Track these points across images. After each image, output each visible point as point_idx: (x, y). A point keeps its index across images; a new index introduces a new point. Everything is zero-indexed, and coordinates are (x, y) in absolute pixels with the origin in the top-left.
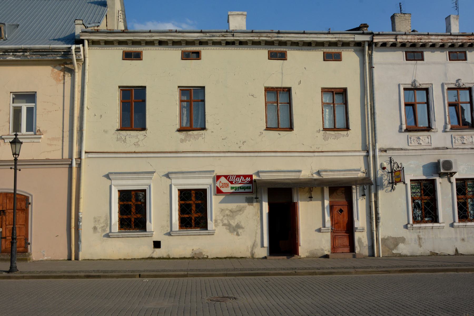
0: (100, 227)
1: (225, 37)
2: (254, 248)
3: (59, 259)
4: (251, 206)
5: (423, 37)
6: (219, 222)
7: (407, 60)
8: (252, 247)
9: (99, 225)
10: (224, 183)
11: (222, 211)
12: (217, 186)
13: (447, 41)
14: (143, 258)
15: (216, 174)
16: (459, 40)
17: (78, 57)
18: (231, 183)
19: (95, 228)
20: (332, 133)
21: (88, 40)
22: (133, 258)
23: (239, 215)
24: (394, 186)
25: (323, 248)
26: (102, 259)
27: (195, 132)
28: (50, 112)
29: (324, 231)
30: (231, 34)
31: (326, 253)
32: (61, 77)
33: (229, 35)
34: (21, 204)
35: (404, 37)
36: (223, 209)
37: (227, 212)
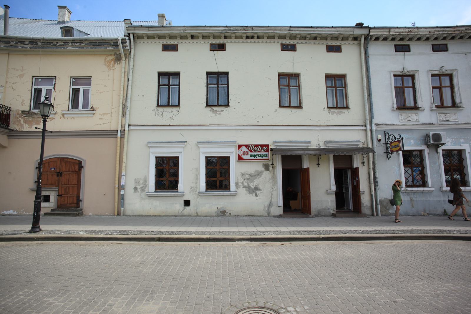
0: (140, 187)
1: (246, 30)
2: (270, 207)
4: (267, 171)
5: (413, 29)
6: (240, 185)
7: (396, 51)
8: (268, 206)
9: (139, 186)
10: (245, 152)
13: (434, 33)
16: (445, 32)
18: (251, 151)
19: (135, 188)
20: (335, 110)
21: (133, 34)
23: (257, 179)
24: (390, 155)
25: (330, 208)
29: (330, 193)
30: (251, 28)
31: (332, 212)
33: (249, 29)
34: (74, 167)
35: (397, 30)
36: (243, 173)
37: (247, 176)
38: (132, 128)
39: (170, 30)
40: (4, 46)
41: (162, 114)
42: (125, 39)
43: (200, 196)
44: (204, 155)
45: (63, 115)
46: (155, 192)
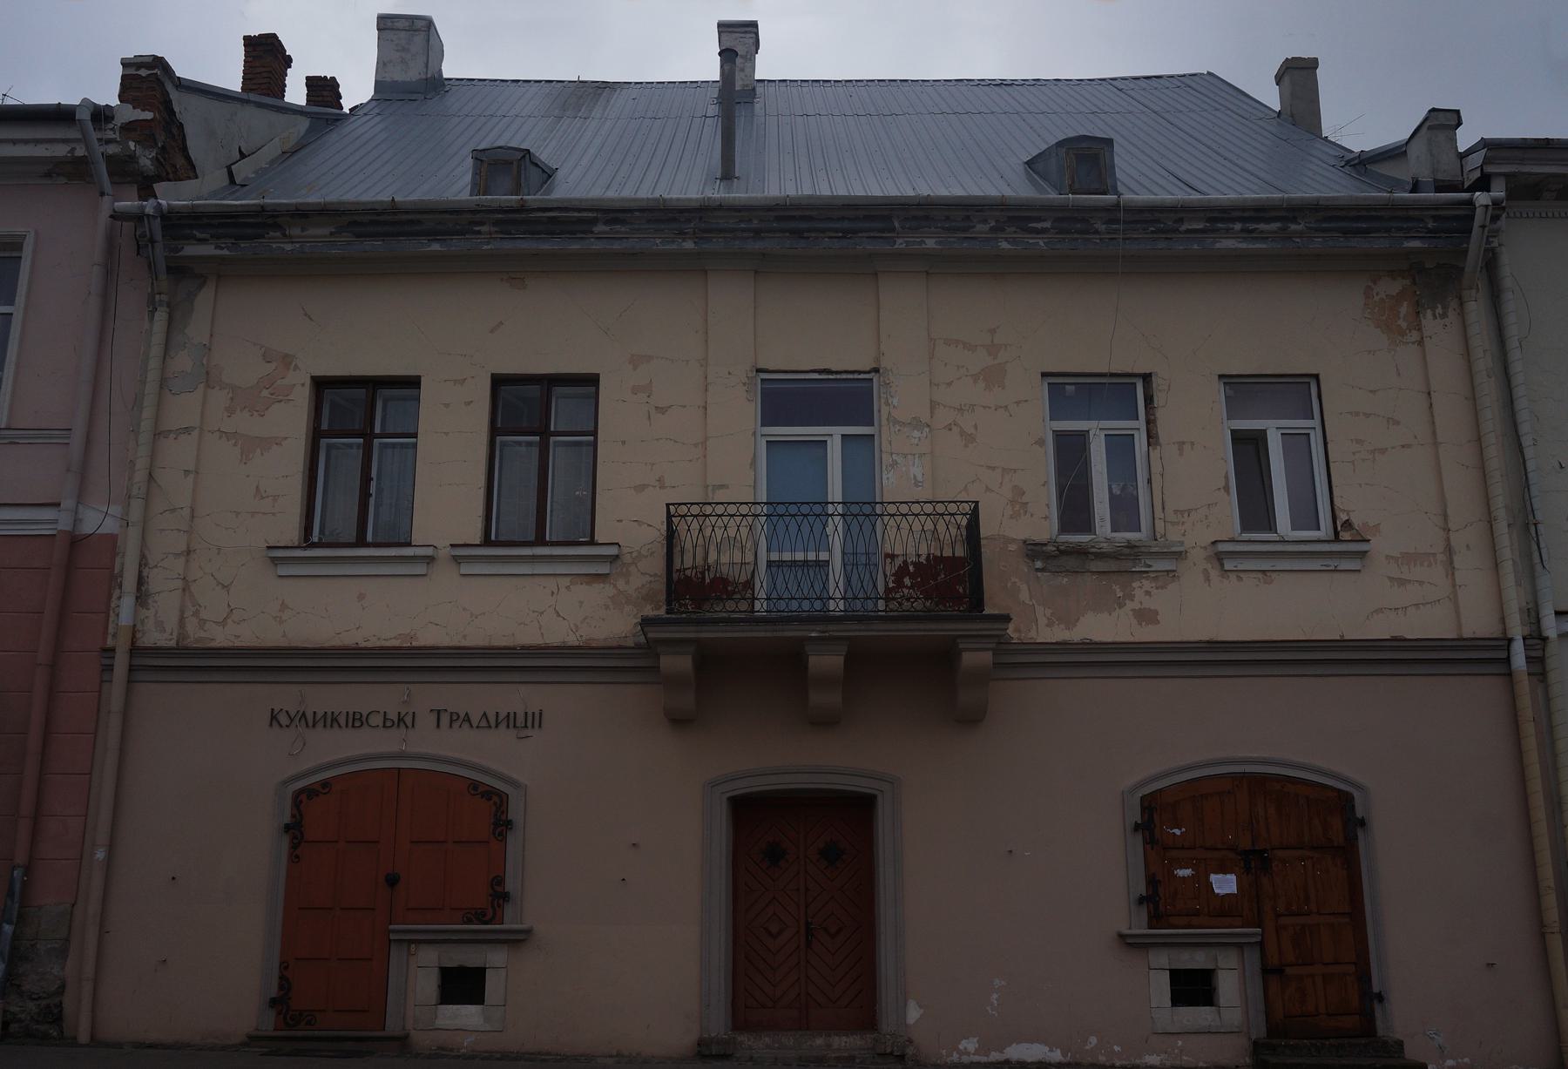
28: (1383, 451)
45: (1220, 558)
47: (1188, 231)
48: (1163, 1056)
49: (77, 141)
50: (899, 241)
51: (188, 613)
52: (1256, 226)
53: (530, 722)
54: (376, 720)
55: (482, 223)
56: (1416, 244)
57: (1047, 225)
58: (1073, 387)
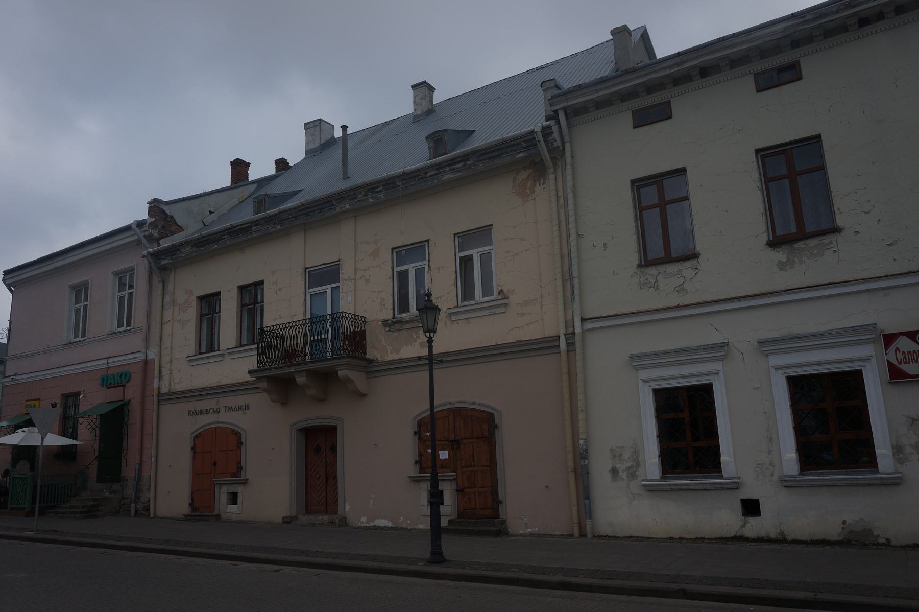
1: (854, 7)
3: (553, 534)
9: (623, 464)
10: (909, 352)
11: (912, 424)
12: (887, 360)
14: (721, 539)
15: (883, 331)
17: (550, 144)
19: (614, 472)
21: (565, 109)
22: (699, 537)
26: (634, 537)
27: (813, 242)
32: (529, 189)
38: (589, 325)
39: (646, 74)
40: (349, 206)
41: (656, 282)
42: (549, 127)
43: (786, 487)
44: (783, 374)
46: (663, 478)
47: (430, 176)
48: (424, 525)
49: (134, 235)
50: (338, 208)
51: (172, 381)
52: (454, 167)
53: (247, 407)
54: (211, 411)
55: (224, 235)
56: (522, 155)
57: (381, 188)
58: (404, 251)
